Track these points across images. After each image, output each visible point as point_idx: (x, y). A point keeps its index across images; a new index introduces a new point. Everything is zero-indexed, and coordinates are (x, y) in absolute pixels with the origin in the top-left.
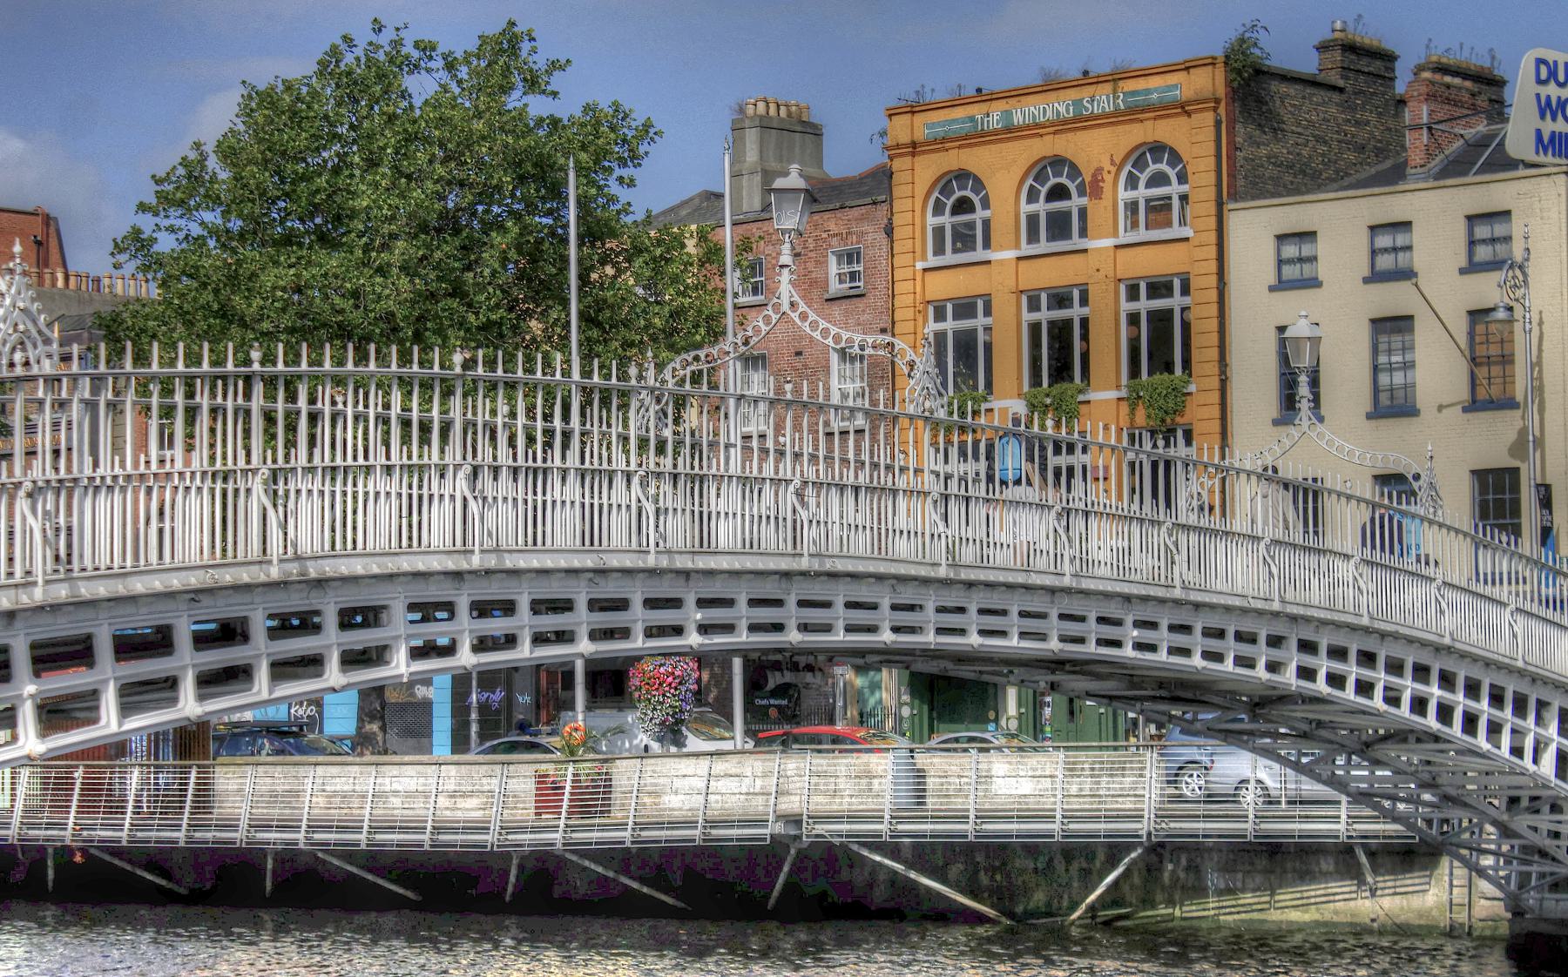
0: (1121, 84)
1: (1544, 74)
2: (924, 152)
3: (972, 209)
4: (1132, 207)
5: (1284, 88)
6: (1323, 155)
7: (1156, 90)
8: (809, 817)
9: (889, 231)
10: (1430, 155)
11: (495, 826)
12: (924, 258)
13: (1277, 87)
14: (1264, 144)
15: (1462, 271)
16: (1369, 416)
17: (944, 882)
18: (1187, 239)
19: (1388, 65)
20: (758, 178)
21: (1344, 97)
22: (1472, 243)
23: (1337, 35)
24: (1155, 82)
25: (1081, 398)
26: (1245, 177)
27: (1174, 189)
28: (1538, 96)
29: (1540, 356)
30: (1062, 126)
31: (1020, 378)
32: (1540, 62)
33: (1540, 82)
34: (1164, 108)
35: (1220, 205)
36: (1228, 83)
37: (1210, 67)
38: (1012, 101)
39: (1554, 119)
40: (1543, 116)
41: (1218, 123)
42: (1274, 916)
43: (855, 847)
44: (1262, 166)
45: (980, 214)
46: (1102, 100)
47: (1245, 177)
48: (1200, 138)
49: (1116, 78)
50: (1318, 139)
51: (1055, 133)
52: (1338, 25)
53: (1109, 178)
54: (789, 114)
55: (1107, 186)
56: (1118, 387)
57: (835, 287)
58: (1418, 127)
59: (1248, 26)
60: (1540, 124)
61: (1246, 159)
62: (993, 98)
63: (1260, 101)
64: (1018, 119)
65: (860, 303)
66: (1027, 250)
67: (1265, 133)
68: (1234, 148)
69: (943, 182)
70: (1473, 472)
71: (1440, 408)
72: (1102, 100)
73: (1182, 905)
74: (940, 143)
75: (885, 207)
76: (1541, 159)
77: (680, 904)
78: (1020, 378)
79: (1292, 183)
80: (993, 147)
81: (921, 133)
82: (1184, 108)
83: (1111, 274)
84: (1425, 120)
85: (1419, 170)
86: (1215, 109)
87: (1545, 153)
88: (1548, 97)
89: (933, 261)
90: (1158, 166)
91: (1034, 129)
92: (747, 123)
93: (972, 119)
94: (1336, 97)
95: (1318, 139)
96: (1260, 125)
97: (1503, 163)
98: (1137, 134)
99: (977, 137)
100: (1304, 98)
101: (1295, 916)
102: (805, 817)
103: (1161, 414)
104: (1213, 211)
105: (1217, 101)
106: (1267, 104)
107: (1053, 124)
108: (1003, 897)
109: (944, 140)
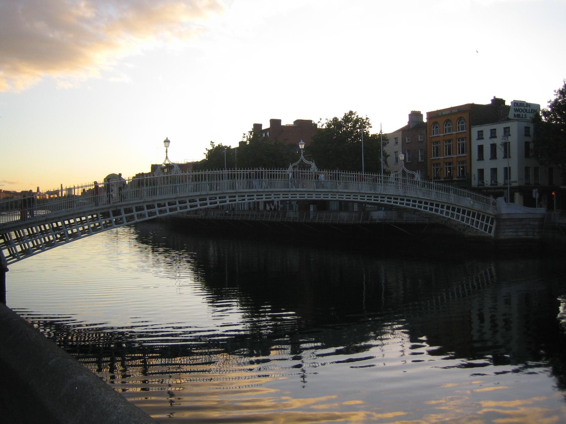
9: (426, 131)
28: (514, 109)
33: (514, 106)
40: (515, 112)
41: (470, 114)
45: (438, 129)
87: (516, 117)
88: (516, 109)
97: (508, 120)
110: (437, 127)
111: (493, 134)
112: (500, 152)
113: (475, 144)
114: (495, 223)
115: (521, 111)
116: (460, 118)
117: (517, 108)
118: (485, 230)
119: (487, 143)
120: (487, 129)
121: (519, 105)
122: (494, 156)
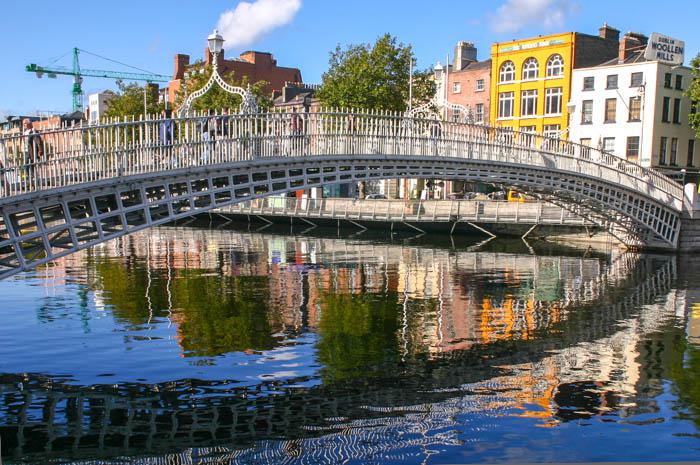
27: (560, 66)
30: (534, 49)
45: (512, 72)
91: (528, 50)
110: (509, 69)
111: (612, 82)
112: (622, 112)
113: (579, 96)
114: (679, 225)
116: (552, 57)
119: (599, 94)
120: (600, 73)
122: (609, 118)
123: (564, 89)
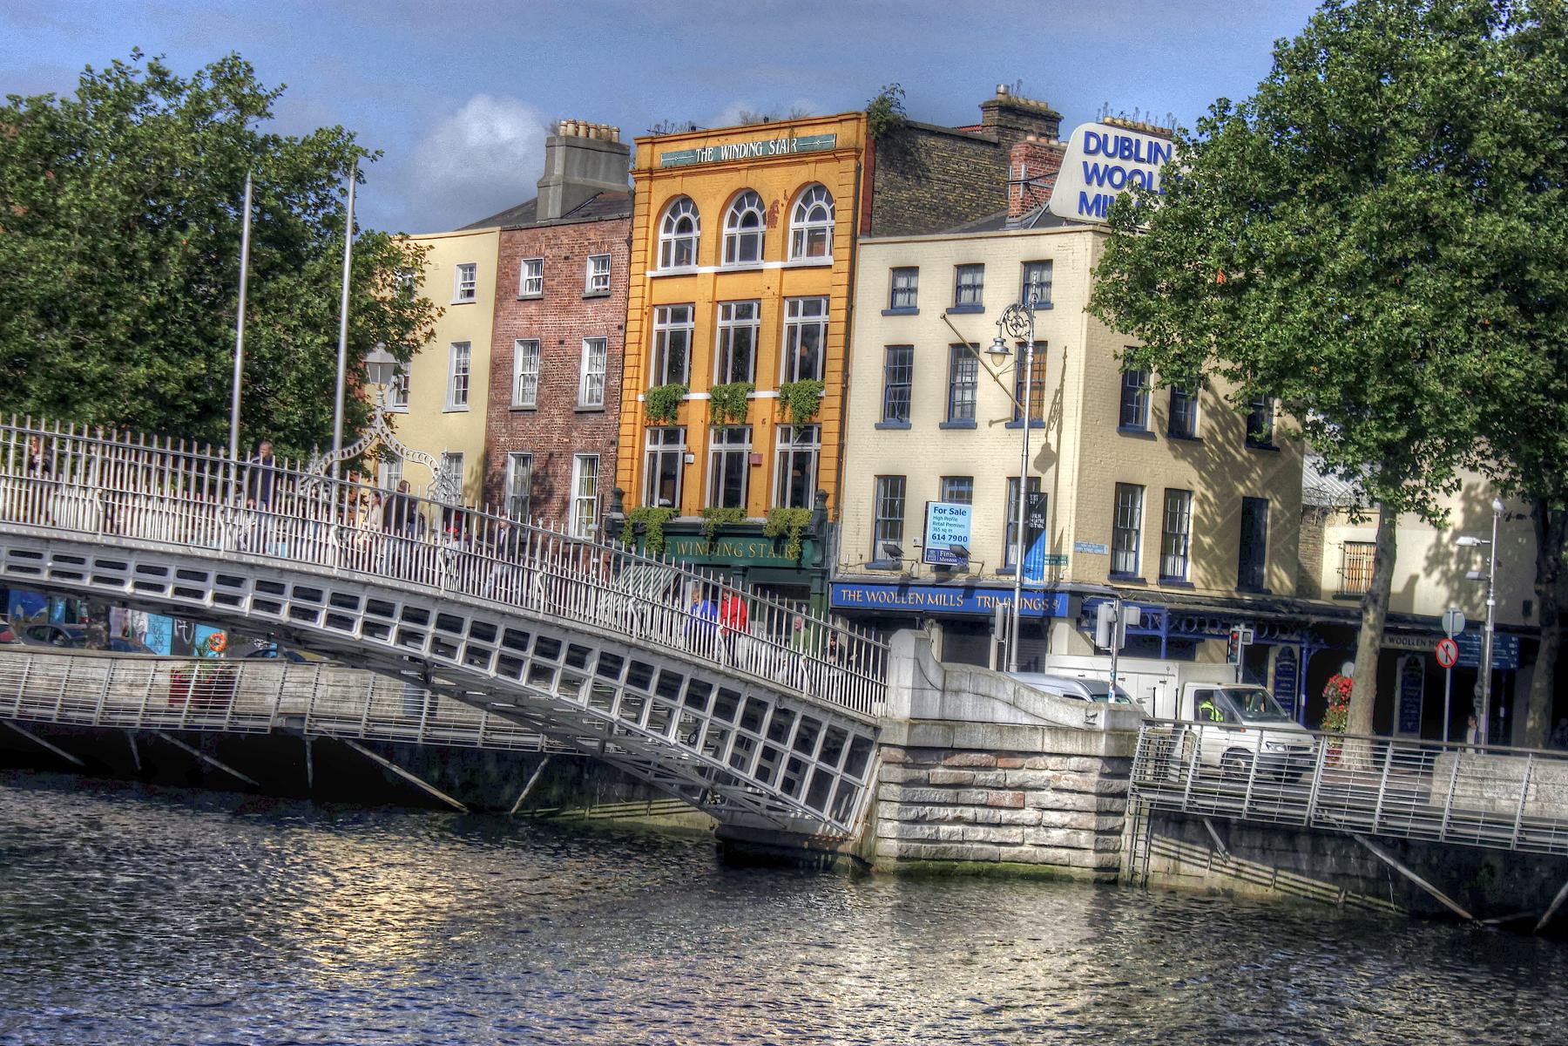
0: (796, 130)
1: (1093, 143)
2: (660, 178)
3: (690, 230)
4: (798, 235)
5: (932, 142)
6: (972, 200)
7: (819, 137)
8: (312, 716)
9: (629, 242)
10: (1024, 208)
11: (99, 708)
12: (654, 268)
13: (922, 140)
14: (905, 188)
15: (884, 313)
16: (942, 427)
17: (424, 779)
18: (830, 266)
19: (1051, 124)
20: (560, 190)
21: (999, 151)
22: (959, 288)
23: (1000, 97)
24: (819, 131)
25: (749, 395)
26: (883, 217)
27: (827, 223)
28: (1085, 164)
29: (1062, 385)
30: (755, 163)
31: (710, 374)
32: (1089, 135)
33: (1087, 151)
34: (822, 153)
35: (854, 238)
36: (868, 136)
37: (855, 122)
38: (722, 139)
39: (1100, 184)
40: (1089, 181)
41: (858, 170)
42: (649, 821)
43: (350, 743)
44: (902, 208)
45: (696, 233)
46: (780, 143)
47: (883, 217)
48: (844, 181)
49: (793, 124)
50: (966, 187)
51: (748, 169)
52: (1002, 89)
53: (782, 210)
54: (598, 136)
55: (780, 216)
56: (775, 388)
57: (591, 287)
58: (1016, 183)
59: (888, 88)
60: (1085, 188)
61: (883, 201)
62: (708, 135)
63: (905, 152)
64: (725, 155)
65: (606, 303)
66: (725, 266)
67: (907, 179)
68: (872, 191)
69: (670, 207)
70: (879, 477)
71: (991, 423)
72: (780, 143)
73: (591, 807)
74: (670, 171)
75: (628, 222)
76: (1085, 217)
77: (78, 761)
78: (710, 374)
79: (934, 223)
80: (706, 177)
81: (659, 162)
82: (833, 154)
83: (777, 293)
84: (1022, 178)
85: (1015, 219)
86: (857, 158)
87: (1089, 213)
88: (1096, 166)
89: (661, 270)
90: (819, 202)
92: (557, 142)
93: (693, 152)
94: (989, 151)
95: (966, 187)
96: (902, 172)
97: (1050, 220)
98: (736, 180)
99: (696, 168)
100: (954, 150)
101: (661, 821)
102: (308, 717)
103: (800, 414)
104: (848, 244)
105: (858, 150)
106: (912, 154)
107: (746, 161)
108: (465, 790)
109: (671, 169)
115: (1117, 178)
117: (1101, 160)
118: (817, 798)
121: (1111, 149)
123: (834, 304)
